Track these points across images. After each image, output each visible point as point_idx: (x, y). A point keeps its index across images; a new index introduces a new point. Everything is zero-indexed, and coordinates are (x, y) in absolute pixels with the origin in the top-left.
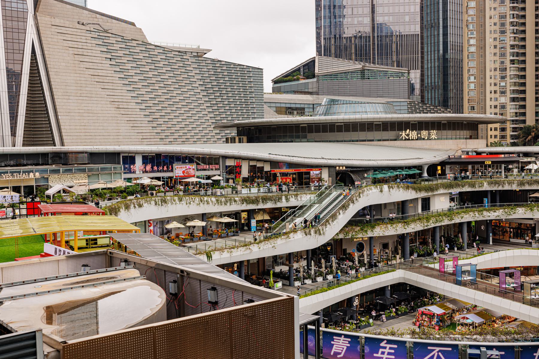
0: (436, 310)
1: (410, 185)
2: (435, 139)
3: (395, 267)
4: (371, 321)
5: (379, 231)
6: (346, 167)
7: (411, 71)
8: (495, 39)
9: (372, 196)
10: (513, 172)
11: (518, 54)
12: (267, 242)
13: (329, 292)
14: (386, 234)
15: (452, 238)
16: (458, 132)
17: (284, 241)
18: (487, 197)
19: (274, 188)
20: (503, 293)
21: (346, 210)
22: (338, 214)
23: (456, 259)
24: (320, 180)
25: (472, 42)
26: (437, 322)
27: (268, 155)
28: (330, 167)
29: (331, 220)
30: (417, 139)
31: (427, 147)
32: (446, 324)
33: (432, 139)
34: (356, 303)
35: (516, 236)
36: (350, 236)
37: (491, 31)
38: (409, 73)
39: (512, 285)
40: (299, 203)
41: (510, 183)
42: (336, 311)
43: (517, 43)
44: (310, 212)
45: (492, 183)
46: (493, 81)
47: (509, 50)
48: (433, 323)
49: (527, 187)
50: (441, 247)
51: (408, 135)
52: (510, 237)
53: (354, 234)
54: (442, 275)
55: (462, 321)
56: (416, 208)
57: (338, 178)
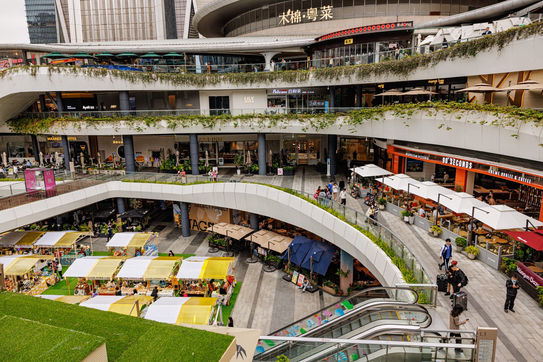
2: (329, 19)
30: (302, 22)
33: (324, 19)
49: (373, 79)
51: (289, 18)
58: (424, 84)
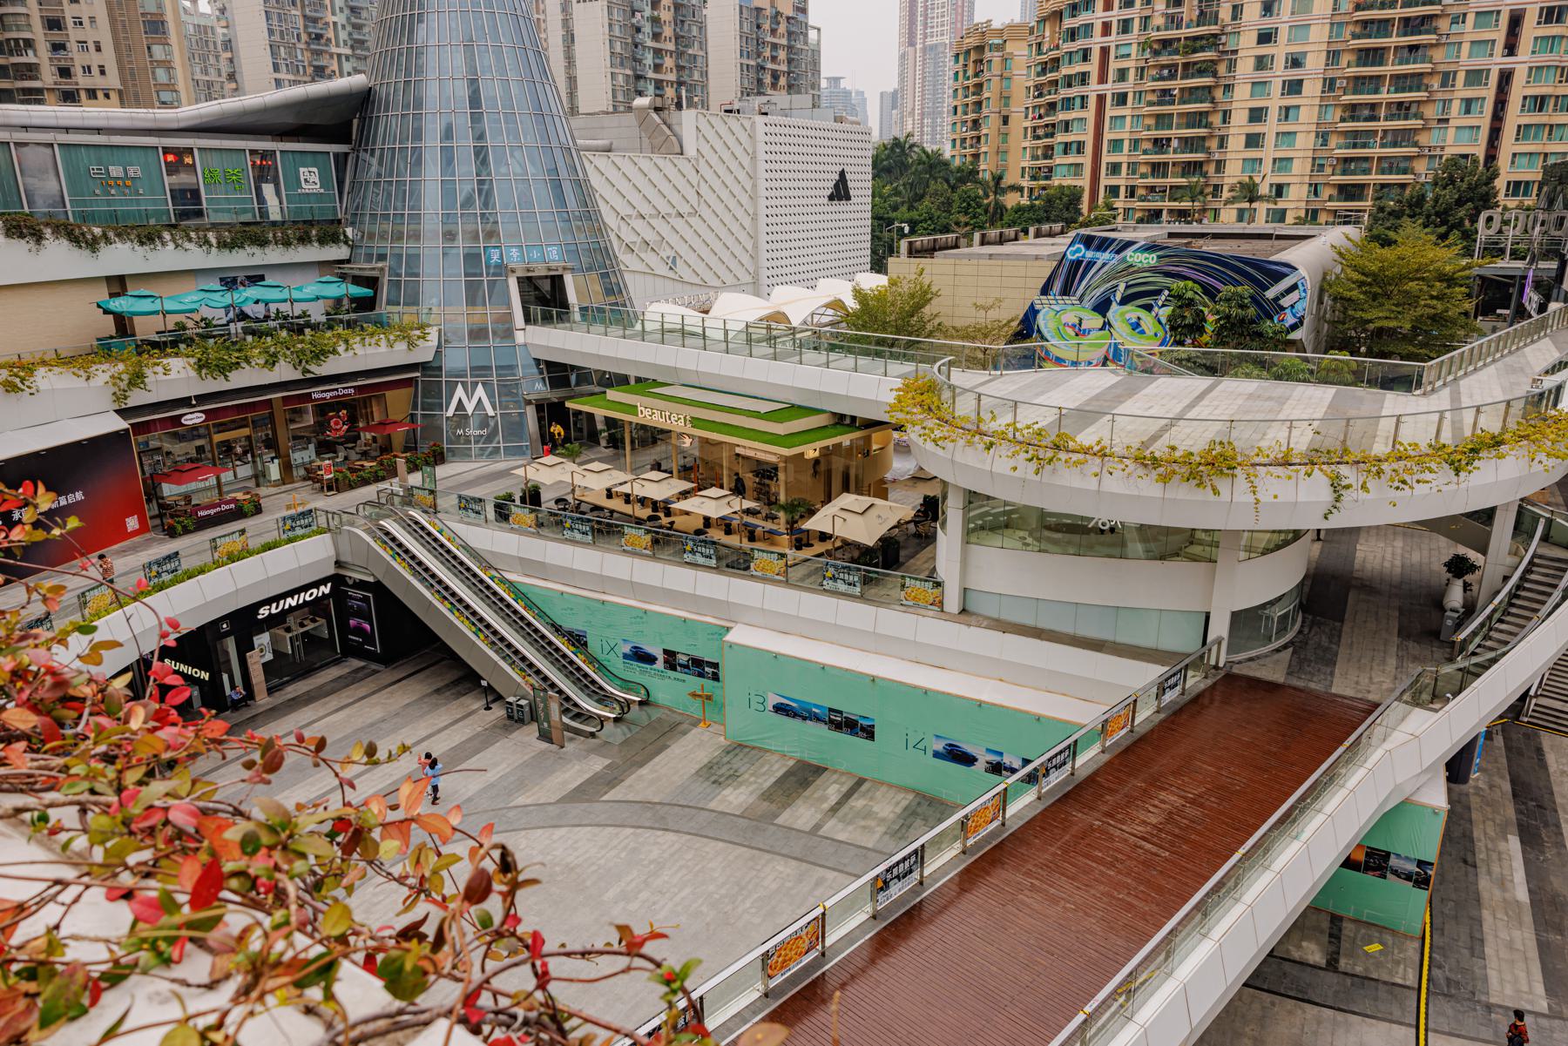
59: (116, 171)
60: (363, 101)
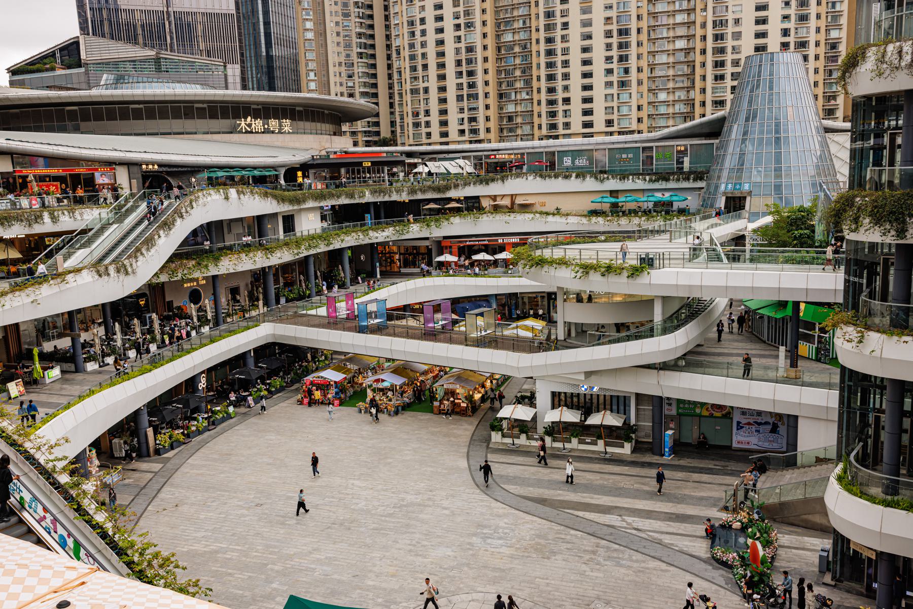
0: (332, 375)
1: (269, 191)
2: (289, 133)
3: (258, 321)
4: (231, 409)
5: (226, 266)
6: (159, 166)
7: (229, 66)
8: (337, 23)
9: (211, 206)
10: (398, 176)
11: (365, 46)
12: (17, 293)
13: (155, 371)
14: (240, 269)
15: (332, 269)
16: (319, 125)
17: (55, 289)
18: (369, 213)
19: (24, 202)
20: (430, 335)
21: (170, 229)
22: (156, 237)
23: (350, 297)
24: (114, 189)
25: (309, 25)
26: (337, 393)
27: (5, 142)
28: (129, 165)
29: (145, 247)
31: (279, 144)
32: (348, 394)
34: (202, 384)
35: (406, 264)
36: (179, 278)
37: (331, 12)
38: (225, 66)
39: (441, 323)
40: (80, 226)
41: (398, 191)
42: (170, 403)
43: (363, 31)
44: (103, 238)
45: (376, 192)
46: (338, 79)
47: (355, 40)
48: (330, 396)
49: (420, 196)
50: (317, 285)
51: (250, 125)
52: (400, 267)
53: (185, 272)
54: (332, 323)
55: (375, 385)
56: (275, 231)
57: (147, 184)
58: (458, 201)
59: (624, 156)
60: (722, 120)
